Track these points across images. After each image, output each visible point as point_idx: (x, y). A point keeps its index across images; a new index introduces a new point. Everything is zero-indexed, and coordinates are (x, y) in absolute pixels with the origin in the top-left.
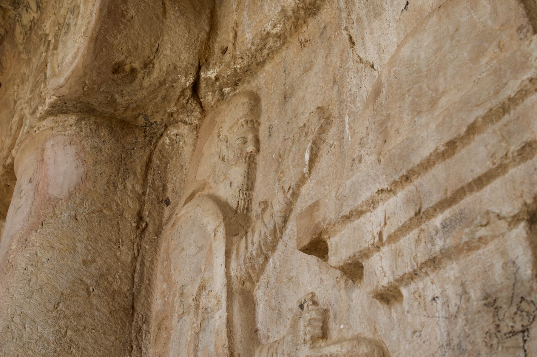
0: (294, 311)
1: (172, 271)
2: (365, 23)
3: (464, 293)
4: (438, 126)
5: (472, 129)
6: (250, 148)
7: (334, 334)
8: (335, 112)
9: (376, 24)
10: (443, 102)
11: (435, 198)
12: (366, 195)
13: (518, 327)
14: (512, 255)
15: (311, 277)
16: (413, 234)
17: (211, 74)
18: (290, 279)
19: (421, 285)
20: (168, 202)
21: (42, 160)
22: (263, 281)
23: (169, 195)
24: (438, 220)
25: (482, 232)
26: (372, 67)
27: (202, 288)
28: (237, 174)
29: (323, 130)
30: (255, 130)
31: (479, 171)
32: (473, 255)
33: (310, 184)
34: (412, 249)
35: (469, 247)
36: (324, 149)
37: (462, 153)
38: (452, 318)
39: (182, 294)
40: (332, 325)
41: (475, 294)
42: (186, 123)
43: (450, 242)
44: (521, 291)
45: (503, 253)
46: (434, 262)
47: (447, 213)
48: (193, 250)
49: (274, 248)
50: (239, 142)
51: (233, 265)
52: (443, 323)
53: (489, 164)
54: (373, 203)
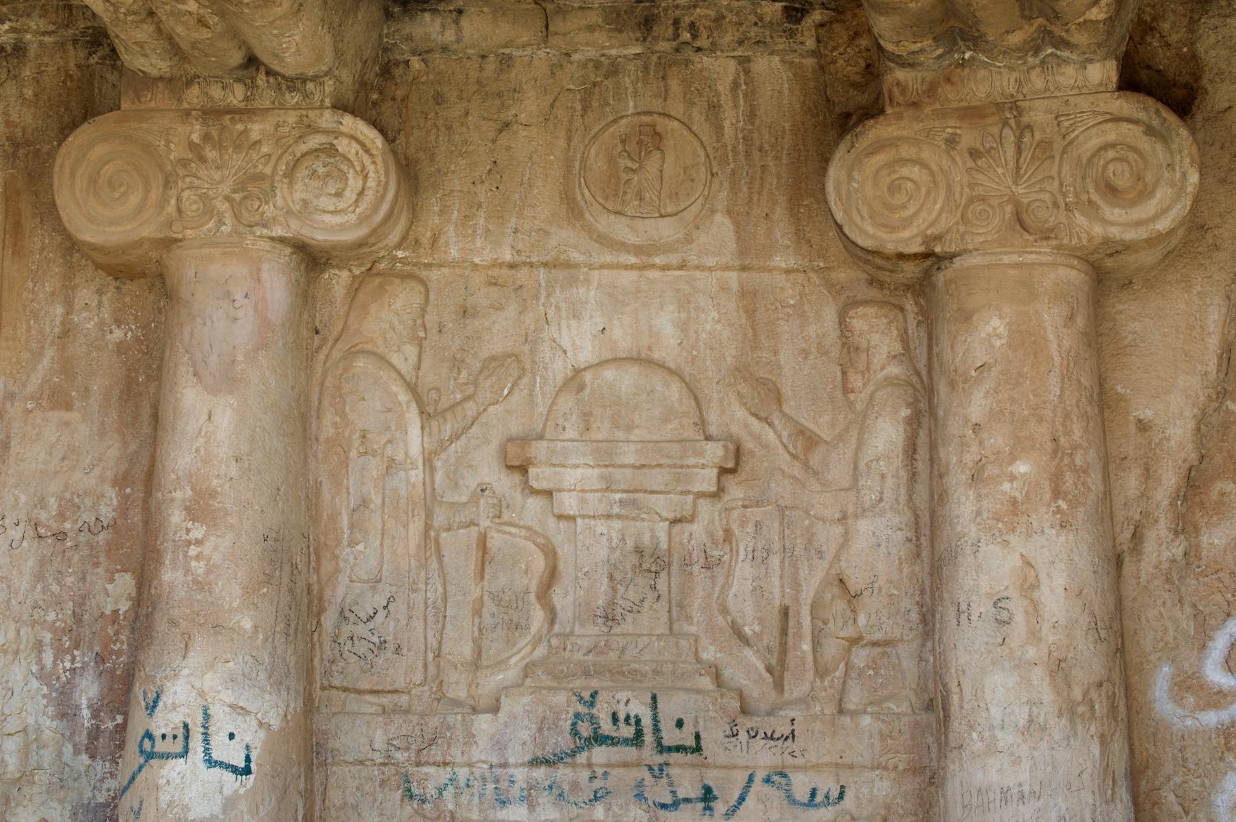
0: (472, 489)
1: (347, 410)
2: (564, 314)
3: (623, 539)
4: (637, 450)
5: (659, 465)
6: (422, 334)
7: (506, 517)
8: (528, 366)
9: (573, 323)
10: (637, 431)
11: (623, 487)
12: (573, 460)
13: (653, 569)
14: (658, 534)
15: (489, 472)
16: (599, 495)
17: (400, 254)
18: (470, 466)
19: (593, 522)
20: (317, 332)
21: (259, 280)
22: (443, 456)
23: (317, 324)
24: (618, 496)
25: (644, 516)
26: (565, 352)
27: (390, 441)
28: (411, 351)
29: (520, 378)
30: (423, 316)
31: (655, 488)
32: (632, 523)
33: (499, 408)
34: (594, 503)
35: (634, 519)
36: (516, 390)
37: (646, 471)
38: (612, 549)
39: (364, 437)
40: (504, 510)
41: (630, 543)
42: (350, 271)
43: (623, 512)
44: (658, 553)
45: (652, 530)
46: (609, 517)
47: (625, 495)
48: (379, 406)
49: (458, 438)
50: (411, 322)
51: (426, 439)
52: (606, 549)
53: (663, 488)
54: (577, 466)
